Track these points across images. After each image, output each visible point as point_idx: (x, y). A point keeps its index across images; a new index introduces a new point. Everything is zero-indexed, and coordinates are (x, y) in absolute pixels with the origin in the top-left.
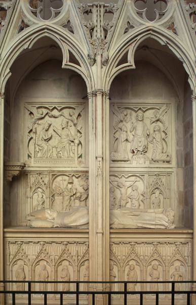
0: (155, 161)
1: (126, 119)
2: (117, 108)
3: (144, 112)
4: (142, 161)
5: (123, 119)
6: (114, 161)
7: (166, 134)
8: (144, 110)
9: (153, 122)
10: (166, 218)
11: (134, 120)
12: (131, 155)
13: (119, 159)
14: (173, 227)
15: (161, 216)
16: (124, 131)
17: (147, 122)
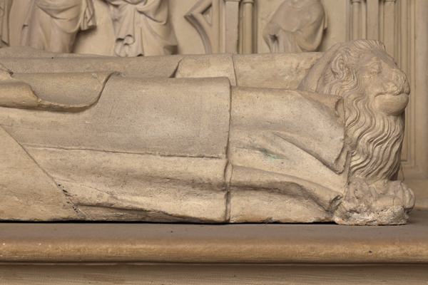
10: (322, 125)
14: (387, 204)
15: (280, 108)
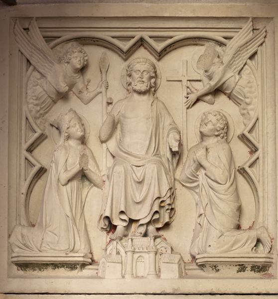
0: (202, 266)
1: (80, 85)
2: (42, 44)
3: (161, 55)
4: (145, 265)
5: (64, 88)
6: (24, 266)
7: (254, 149)
8: (159, 47)
9: (198, 100)
11: (117, 91)
12: (99, 238)
13: (48, 255)
16: (68, 137)
17: (174, 97)
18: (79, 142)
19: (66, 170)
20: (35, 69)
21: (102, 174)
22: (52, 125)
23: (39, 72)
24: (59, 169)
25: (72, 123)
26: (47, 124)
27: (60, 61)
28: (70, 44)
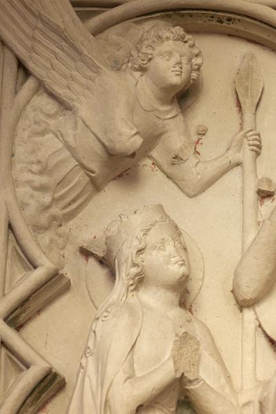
1: (175, 139)
5: (127, 138)
16: (140, 281)
18: (173, 297)
19: (130, 377)
20: (42, 87)
21: (243, 399)
22: (86, 253)
23: (52, 95)
24: (110, 370)
25: (154, 237)
26: (71, 252)
27: (117, 67)
28: (147, 25)
